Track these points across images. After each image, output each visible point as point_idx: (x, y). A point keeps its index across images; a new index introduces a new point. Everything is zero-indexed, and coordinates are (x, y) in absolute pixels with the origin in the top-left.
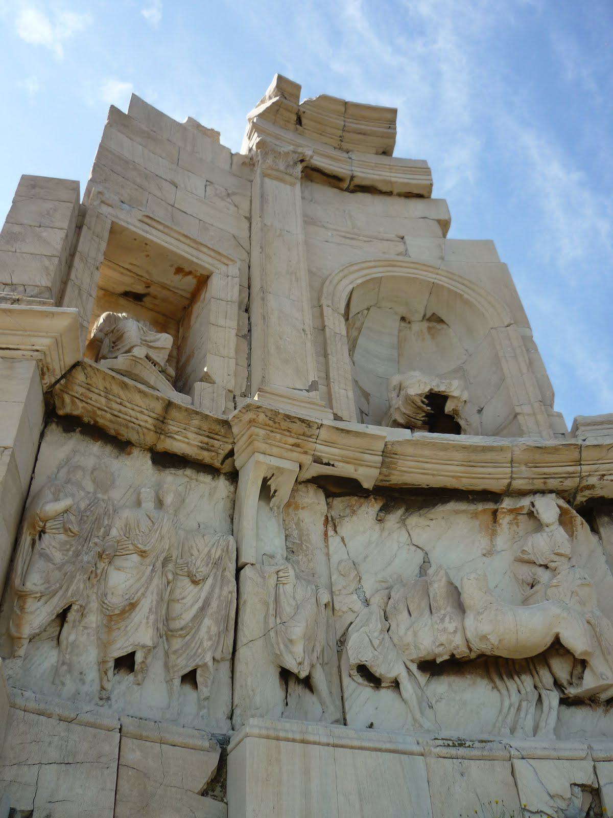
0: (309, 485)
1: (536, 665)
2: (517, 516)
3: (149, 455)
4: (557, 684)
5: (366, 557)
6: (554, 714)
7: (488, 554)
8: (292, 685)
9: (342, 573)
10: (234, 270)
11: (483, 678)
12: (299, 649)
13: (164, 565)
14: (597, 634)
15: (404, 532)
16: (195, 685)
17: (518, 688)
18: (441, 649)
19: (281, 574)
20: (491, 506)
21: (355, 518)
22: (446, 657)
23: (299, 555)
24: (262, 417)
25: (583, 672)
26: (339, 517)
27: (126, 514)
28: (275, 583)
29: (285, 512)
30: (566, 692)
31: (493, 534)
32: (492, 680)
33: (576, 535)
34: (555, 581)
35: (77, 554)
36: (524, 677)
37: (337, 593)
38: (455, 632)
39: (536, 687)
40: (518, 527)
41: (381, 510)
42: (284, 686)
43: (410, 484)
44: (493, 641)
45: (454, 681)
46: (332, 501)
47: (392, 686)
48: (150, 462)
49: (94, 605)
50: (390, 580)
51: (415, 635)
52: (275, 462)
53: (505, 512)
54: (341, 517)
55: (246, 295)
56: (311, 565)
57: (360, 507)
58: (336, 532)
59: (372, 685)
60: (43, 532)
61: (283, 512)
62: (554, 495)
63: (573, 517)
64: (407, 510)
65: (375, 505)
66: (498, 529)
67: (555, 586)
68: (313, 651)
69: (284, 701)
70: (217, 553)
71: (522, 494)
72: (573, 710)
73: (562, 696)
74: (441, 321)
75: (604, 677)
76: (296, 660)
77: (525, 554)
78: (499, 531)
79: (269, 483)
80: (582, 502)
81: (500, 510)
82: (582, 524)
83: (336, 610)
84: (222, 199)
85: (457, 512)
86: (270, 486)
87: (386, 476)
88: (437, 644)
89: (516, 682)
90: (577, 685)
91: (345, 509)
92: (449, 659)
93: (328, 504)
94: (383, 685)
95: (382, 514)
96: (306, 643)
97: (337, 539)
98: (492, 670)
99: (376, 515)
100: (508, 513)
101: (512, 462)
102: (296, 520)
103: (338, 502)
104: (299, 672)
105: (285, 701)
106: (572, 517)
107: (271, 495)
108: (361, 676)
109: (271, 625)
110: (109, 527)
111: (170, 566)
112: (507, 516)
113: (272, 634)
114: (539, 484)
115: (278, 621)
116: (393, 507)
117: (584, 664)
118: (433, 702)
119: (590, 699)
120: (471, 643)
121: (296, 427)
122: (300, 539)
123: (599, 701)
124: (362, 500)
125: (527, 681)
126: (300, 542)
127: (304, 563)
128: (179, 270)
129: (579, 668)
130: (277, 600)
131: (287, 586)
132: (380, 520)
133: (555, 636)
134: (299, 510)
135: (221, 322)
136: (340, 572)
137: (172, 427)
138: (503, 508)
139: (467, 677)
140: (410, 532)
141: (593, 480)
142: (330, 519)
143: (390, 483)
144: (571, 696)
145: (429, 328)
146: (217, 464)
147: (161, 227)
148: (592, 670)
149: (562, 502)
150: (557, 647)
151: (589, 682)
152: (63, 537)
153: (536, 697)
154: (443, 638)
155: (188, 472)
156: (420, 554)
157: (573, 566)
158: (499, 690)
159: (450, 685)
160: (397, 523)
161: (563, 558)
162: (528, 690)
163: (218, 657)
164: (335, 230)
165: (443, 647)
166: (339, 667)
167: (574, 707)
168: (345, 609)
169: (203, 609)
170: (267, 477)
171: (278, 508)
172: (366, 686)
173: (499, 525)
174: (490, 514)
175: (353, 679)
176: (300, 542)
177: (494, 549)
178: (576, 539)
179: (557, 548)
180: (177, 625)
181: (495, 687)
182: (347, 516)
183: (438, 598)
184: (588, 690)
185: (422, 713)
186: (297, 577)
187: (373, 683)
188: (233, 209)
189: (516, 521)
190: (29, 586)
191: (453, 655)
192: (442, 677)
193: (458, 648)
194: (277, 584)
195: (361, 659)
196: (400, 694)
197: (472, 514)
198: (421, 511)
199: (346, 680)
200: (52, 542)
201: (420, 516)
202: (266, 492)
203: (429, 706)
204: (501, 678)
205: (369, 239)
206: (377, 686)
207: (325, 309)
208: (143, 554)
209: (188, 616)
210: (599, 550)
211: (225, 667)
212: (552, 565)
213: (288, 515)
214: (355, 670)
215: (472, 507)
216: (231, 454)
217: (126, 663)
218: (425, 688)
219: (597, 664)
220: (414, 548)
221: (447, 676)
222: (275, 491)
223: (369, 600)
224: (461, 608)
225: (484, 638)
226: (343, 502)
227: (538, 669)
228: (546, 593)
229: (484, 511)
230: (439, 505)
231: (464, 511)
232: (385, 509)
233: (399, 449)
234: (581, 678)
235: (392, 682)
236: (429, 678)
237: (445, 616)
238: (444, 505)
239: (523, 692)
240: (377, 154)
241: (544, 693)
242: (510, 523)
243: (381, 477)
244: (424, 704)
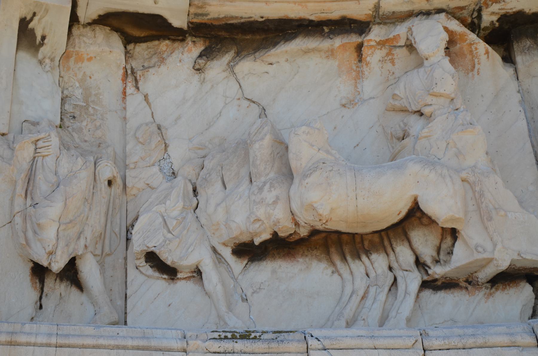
0: (98, 28)
1: (392, 240)
2: (390, 50)
4: (419, 263)
5: (178, 118)
6: (411, 300)
8: (49, 282)
9: (141, 140)
11: (320, 260)
12: (50, 233)
14: (477, 194)
17: (366, 270)
18: (257, 225)
19: (40, 144)
20: (355, 39)
21: (163, 68)
22: (266, 236)
23: (82, 121)
25: (453, 245)
26: (142, 68)
28: (32, 155)
29: (64, 67)
30: (430, 272)
31: (359, 76)
32: (333, 264)
33: (479, 69)
34: (426, 130)
36: (374, 256)
37: (132, 166)
38: (275, 203)
39: (390, 269)
40: (394, 65)
41: (201, 56)
42: (38, 284)
43: (236, 18)
44: (321, 211)
45: (280, 266)
46: (134, 48)
47: (194, 277)
50: (210, 146)
51: (227, 212)
53: (372, 46)
56: (99, 133)
57: (171, 53)
58: (138, 88)
59: (165, 276)
61: (61, 67)
62: (443, 15)
63: (473, 44)
64: (238, 54)
65: (193, 49)
66: (365, 69)
67: (425, 137)
68: (79, 238)
69: (36, 303)
72: (441, 294)
73: (426, 278)
75: (480, 249)
76: (45, 249)
77: (397, 100)
78: (366, 73)
79: (31, 26)
80: (493, 22)
81: (365, 44)
82: (487, 52)
83: (129, 188)
85: (307, 52)
86: (32, 31)
87: (201, 7)
88: (252, 220)
89: (363, 263)
90: (445, 262)
91: (151, 58)
92: (271, 239)
93: (127, 53)
94: (179, 275)
95: (201, 61)
96: (62, 227)
97: (140, 97)
98: (333, 250)
99: (193, 63)
100: (380, 47)
102: (80, 76)
103: (140, 49)
104: (50, 264)
105: (39, 303)
106: (471, 44)
107: (38, 42)
108: (151, 267)
109: (17, 209)
112: (377, 50)
113: (18, 219)
115: (29, 202)
116: (219, 50)
117: (454, 233)
118: (249, 294)
119: (468, 281)
120: (297, 216)
122: (87, 101)
123: (478, 281)
124: (176, 44)
126: (85, 104)
127: (89, 131)
129: (449, 240)
130: (30, 179)
131: (47, 159)
132: (198, 70)
133: (413, 199)
134: (83, 62)
136: (137, 138)
138: (371, 40)
139: (298, 261)
140: (241, 82)
142: (129, 72)
143: (209, 17)
144: (437, 277)
148: (466, 243)
149: (455, 26)
153: (390, 280)
154: (261, 212)
156: (256, 110)
157: (457, 109)
158: (340, 275)
159: (274, 272)
160: (224, 71)
161: (442, 100)
162: (379, 271)
165: (260, 223)
166: (126, 259)
167: (443, 291)
168: (141, 185)
170: (25, 18)
171: (52, 60)
172: (158, 278)
173: (367, 64)
174: (353, 49)
175: (140, 271)
176: (85, 104)
177: (358, 97)
178: (478, 74)
179: (434, 86)
181: (336, 271)
182: (154, 66)
183: (258, 162)
184: (458, 268)
185: (230, 307)
186: (64, 146)
187: (167, 274)
189: (390, 57)
191: (275, 234)
192: (264, 263)
193: (279, 222)
194: (34, 158)
195: (148, 245)
196: (203, 285)
197: (327, 51)
198: (257, 54)
199: (132, 273)
201: (255, 61)
203: (243, 300)
204: (344, 259)
206: (173, 277)
210: (513, 85)
212: (426, 110)
213: (69, 69)
214: (143, 260)
215: (326, 44)
218: (240, 277)
220: (247, 103)
221: (271, 261)
222: (43, 38)
223: (178, 173)
225: (312, 208)
226: (150, 48)
227: (394, 246)
228: (414, 148)
229: (343, 46)
230: (282, 43)
231: (314, 50)
234: (450, 253)
235: (192, 272)
236: (247, 264)
237: (265, 183)
238: (288, 43)
239: (372, 274)
241: (400, 274)
242: (382, 61)
243: (193, 10)
244: (237, 297)
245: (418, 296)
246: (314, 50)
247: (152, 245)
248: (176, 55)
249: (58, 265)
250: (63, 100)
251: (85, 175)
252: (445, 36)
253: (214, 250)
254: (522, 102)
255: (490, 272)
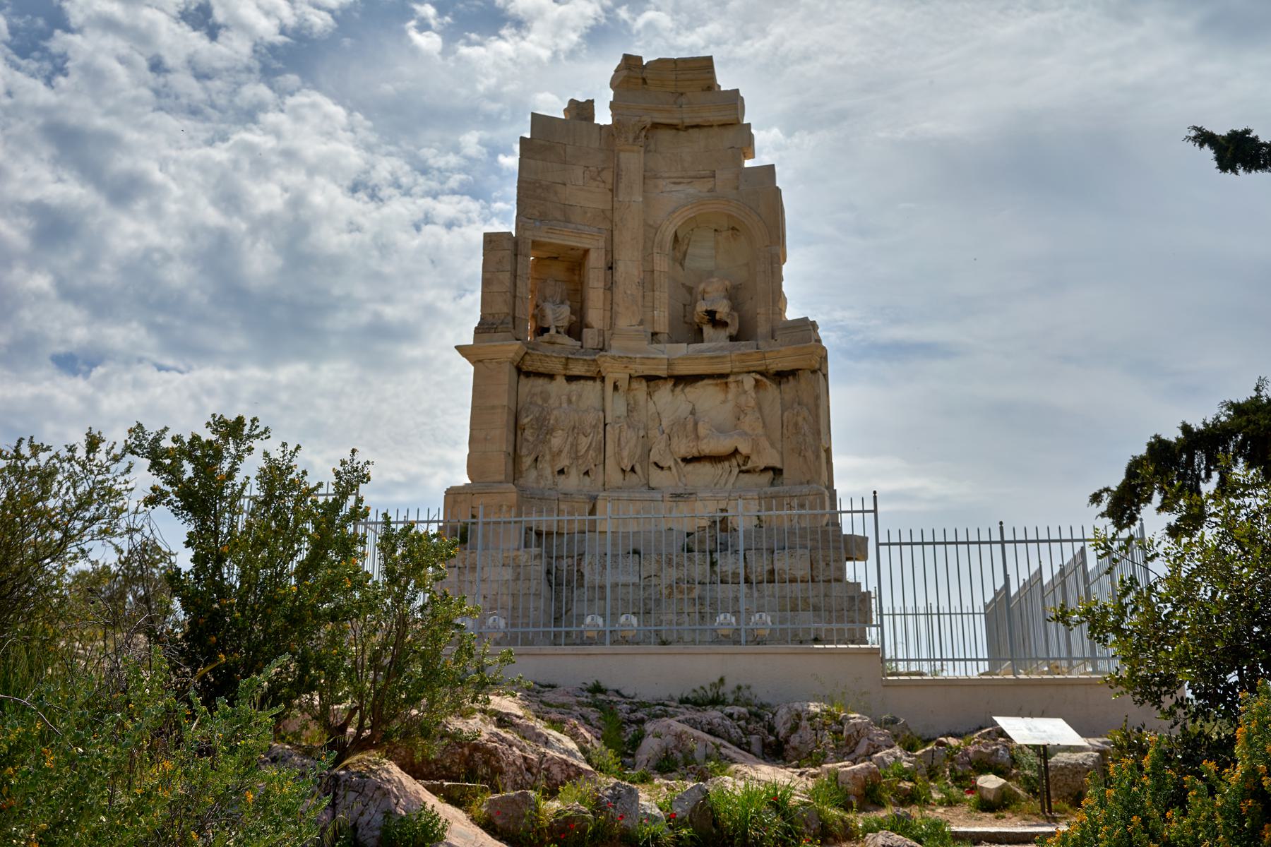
3: (563, 378)
4: (739, 465)
7: (724, 402)
10: (602, 244)
12: (626, 461)
13: (573, 430)
15: (683, 395)
16: (589, 476)
20: (725, 380)
24: (608, 359)
27: (555, 412)
31: (727, 392)
35: (538, 436)
48: (565, 381)
49: (547, 452)
51: (679, 448)
52: (617, 376)
54: (654, 392)
55: (610, 256)
60: (524, 429)
70: (594, 423)
71: (739, 373)
74: (738, 230)
84: (595, 180)
101: (731, 361)
103: (652, 384)
110: (549, 419)
111: (576, 431)
114: (745, 370)
121: (625, 360)
125: (727, 464)
128: (572, 249)
130: (619, 440)
135: (596, 286)
137: (571, 366)
141: (771, 366)
145: (732, 235)
146: (594, 375)
147: (558, 232)
149: (758, 377)
150: (736, 452)
151: (749, 465)
152: (531, 431)
154: (689, 450)
155: (582, 382)
156: (691, 405)
163: (597, 463)
164: (669, 178)
169: (589, 447)
180: (579, 454)
185: (680, 480)
188: (602, 185)
190: (523, 454)
200: (528, 433)
202: (616, 388)
205: (689, 180)
207: (655, 254)
208: (563, 430)
209: (584, 450)
211: (602, 466)
215: (715, 382)
216: (600, 371)
217: (561, 472)
219: (753, 457)
224: (697, 437)
225: (703, 450)
229: (721, 383)
232: (675, 385)
233: (676, 362)
240: (703, 90)
245: (738, 475)
246: (712, 384)
247: (656, 460)
248: (663, 389)
249: (629, 468)
250: (628, 405)
251: (635, 438)
252: (754, 382)
253: (675, 460)
254: (781, 403)
255: (757, 470)
